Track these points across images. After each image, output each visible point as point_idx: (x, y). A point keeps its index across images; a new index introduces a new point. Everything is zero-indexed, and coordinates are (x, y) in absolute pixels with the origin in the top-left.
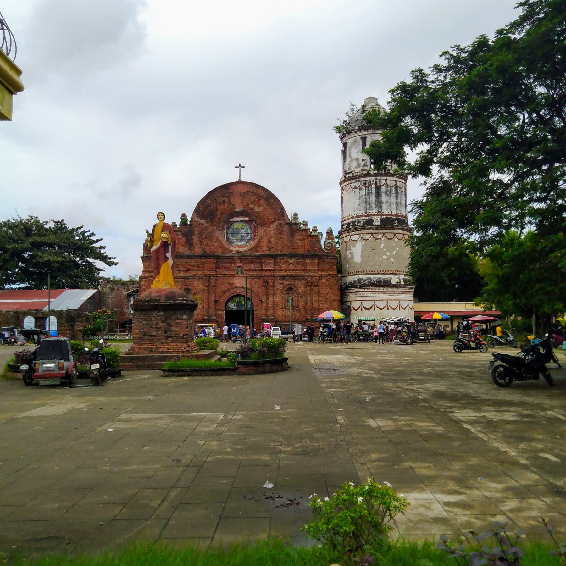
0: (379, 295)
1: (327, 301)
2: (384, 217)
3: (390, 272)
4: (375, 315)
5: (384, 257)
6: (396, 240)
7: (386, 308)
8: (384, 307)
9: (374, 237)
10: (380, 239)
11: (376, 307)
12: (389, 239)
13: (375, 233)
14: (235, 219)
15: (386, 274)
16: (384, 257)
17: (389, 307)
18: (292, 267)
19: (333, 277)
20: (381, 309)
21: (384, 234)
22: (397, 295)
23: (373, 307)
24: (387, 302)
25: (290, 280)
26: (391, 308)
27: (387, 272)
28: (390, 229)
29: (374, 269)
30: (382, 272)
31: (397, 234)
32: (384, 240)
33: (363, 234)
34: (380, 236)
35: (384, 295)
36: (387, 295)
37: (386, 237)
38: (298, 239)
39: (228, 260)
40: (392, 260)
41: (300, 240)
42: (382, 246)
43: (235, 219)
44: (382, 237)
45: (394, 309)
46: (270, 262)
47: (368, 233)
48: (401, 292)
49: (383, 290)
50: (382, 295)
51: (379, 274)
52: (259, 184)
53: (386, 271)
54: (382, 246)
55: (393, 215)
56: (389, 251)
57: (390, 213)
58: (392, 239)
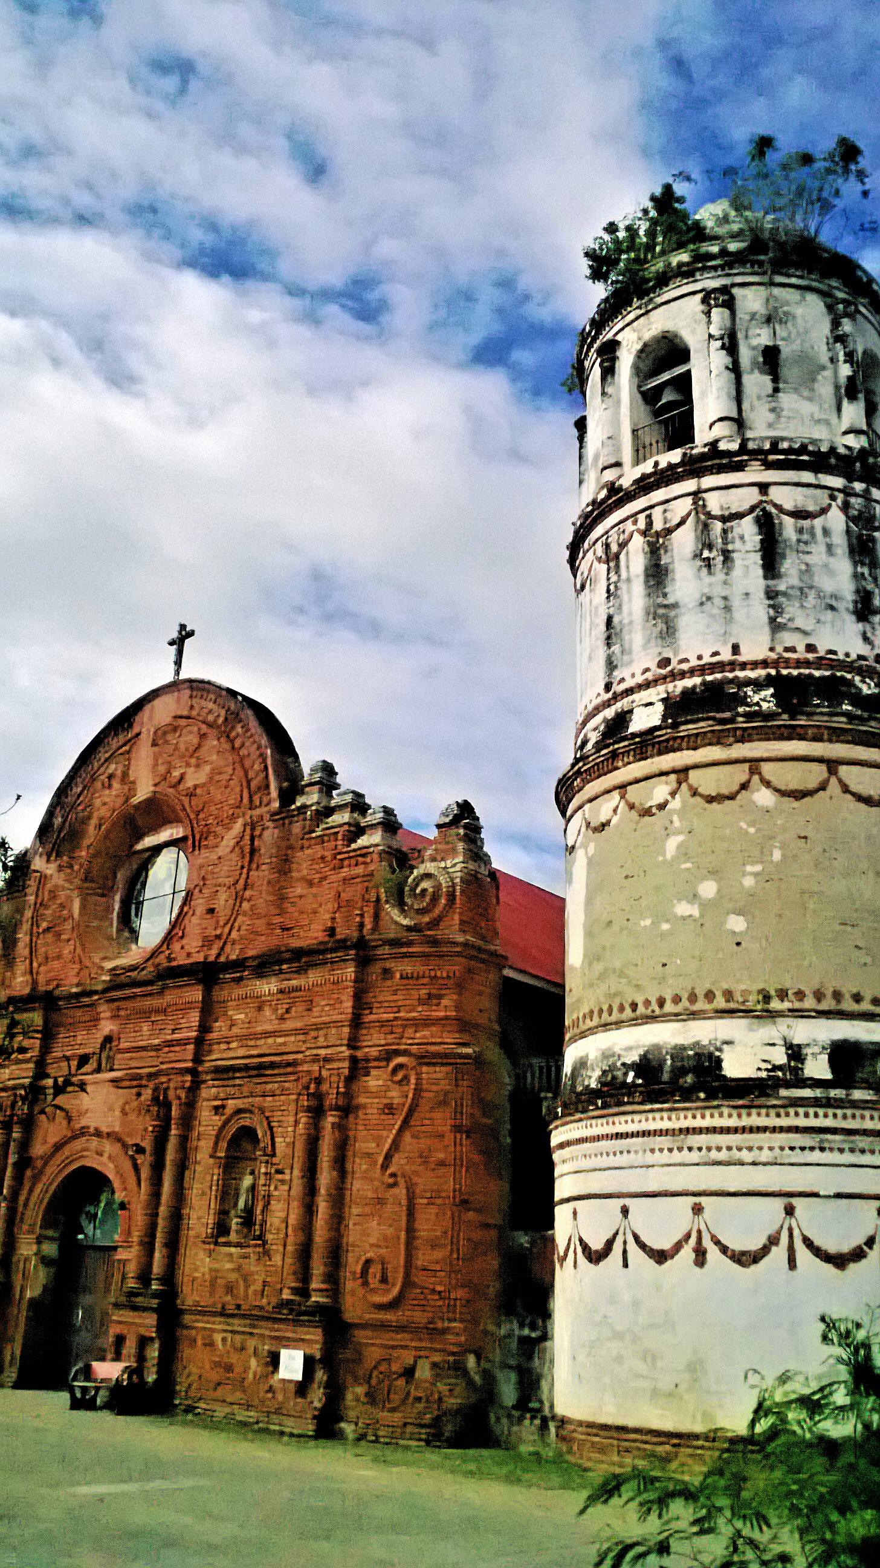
0: (650, 1159)
1: (381, 1201)
2: (697, 680)
3: (720, 1002)
4: (627, 1298)
5: (683, 909)
6: (763, 797)
7: (687, 1253)
8: (678, 1247)
9: (632, 807)
10: (662, 806)
11: (633, 1248)
12: (710, 799)
13: (637, 781)
14: (149, 841)
15: (694, 1015)
16: (683, 909)
17: (707, 1243)
18: (268, 1021)
19: (425, 1059)
20: (661, 1257)
21: (682, 772)
22: (765, 1156)
23: (619, 1240)
24: (698, 1210)
25: (248, 1086)
26: (724, 1249)
27: (701, 1005)
28: (718, 739)
29: (632, 996)
30: (669, 1007)
31: (767, 769)
32: (682, 812)
33: (590, 800)
34: (660, 791)
35: (677, 1157)
36: (695, 1156)
37: (695, 793)
38: (303, 879)
39: (78, 1013)
40: (737, 924)
41: (311, 883)
42: (672, 844)
43: (149, 841)
44: (673, 794)
45: (745, 1259)
46: (187, 1007)
47: (608, 791)
48: (798, 1139)
49: (665, 1125)
50: (665, 1158)
51: (652, 1018)
52: (206, 678)
53: (693, 998)
54: (672, 844)
55: (743, 666)
56: (713, 873)
57: (726, 655)
58: (731, 797)
